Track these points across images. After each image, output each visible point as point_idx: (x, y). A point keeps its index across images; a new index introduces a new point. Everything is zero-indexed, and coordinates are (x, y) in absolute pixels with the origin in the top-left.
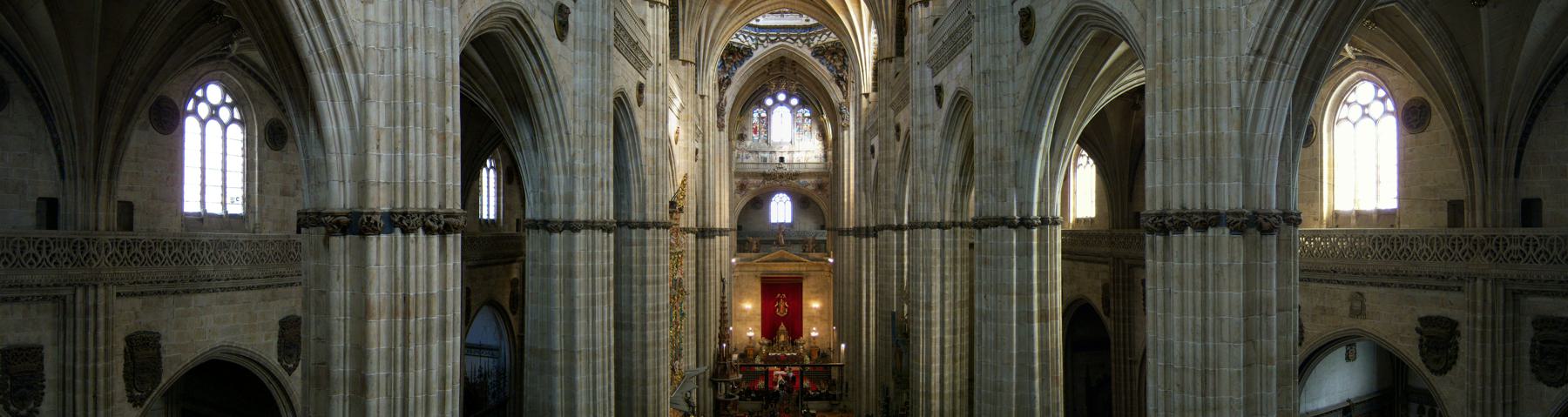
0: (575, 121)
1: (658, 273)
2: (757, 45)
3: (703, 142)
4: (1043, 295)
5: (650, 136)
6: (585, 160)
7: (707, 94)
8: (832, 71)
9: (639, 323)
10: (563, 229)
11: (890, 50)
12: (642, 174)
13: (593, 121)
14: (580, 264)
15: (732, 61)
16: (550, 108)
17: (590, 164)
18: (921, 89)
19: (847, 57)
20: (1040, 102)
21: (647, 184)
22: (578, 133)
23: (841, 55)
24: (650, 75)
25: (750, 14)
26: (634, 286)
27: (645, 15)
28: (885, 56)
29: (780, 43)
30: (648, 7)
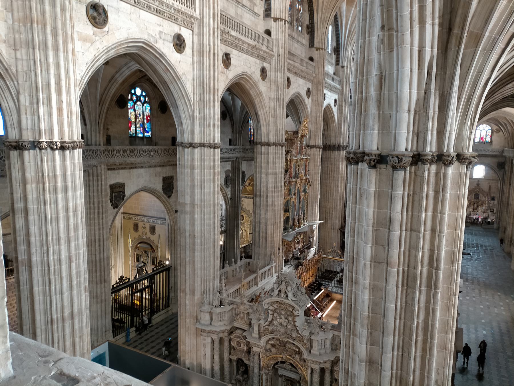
0: (194, 94)
1: (275, 169)
3: (342, 94)
5: (273, 96)
6: (200, 113)
7: (346, 65)
9: (265, 195)
10: (190, 147)
14: (197, 163)
16: (177, 88)
17: (202, 115)
22: (196, 100)
24: (273, 62)
26: (262, 176)
27: (271, 27)
30: (273, 22)
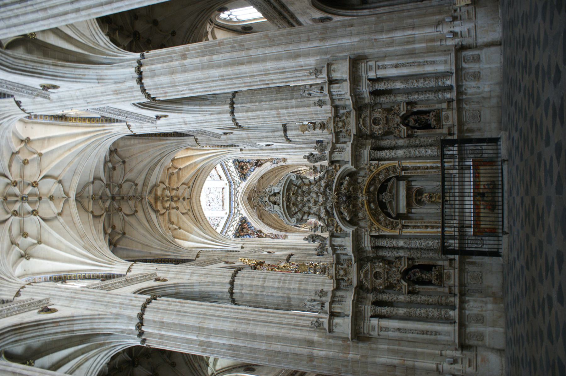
2: (239, 214)
4: (174, 58)
5: (188, 277)
7: (240, 245)
8: (254, 169)
9: (287, 292)
11: (190, 141)
12: (205, 283)
13: (102, 301)
15: (248, 229)
17: (118, 305)
18: (168, 126)
19: (243, 160)
20: (77, 76)
21: (210, 281)
23: (243, 164)
25: (201, 218)
26: (264, 293)
28: (195, 142)
29: (239, 200)
